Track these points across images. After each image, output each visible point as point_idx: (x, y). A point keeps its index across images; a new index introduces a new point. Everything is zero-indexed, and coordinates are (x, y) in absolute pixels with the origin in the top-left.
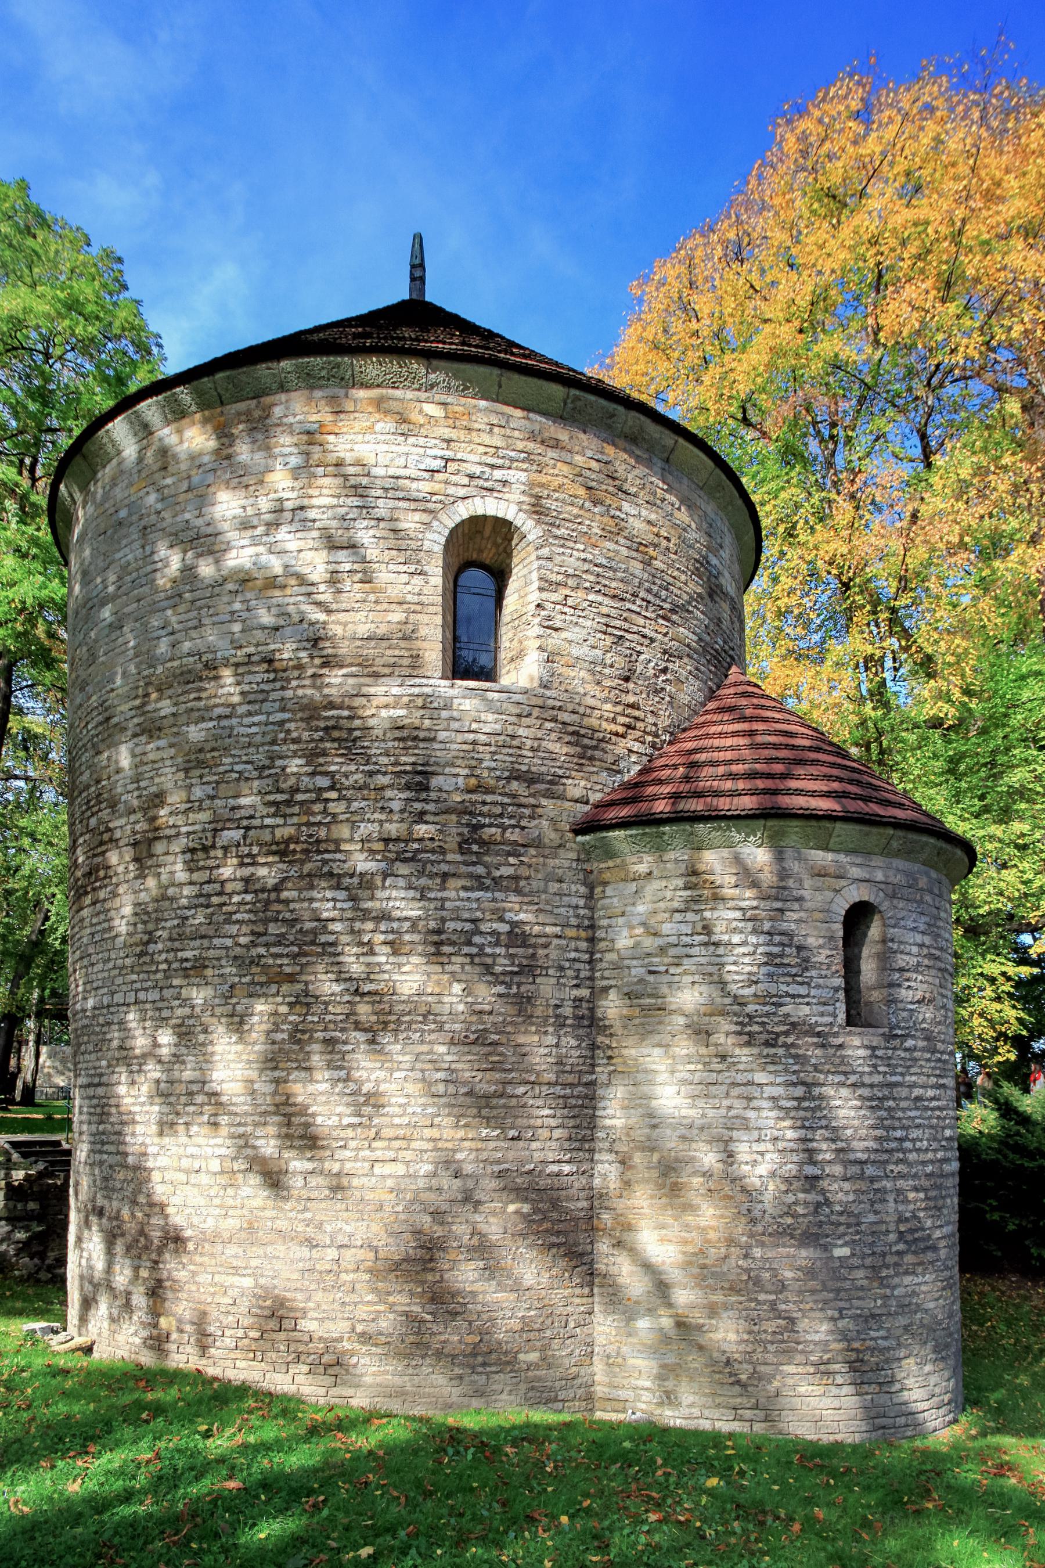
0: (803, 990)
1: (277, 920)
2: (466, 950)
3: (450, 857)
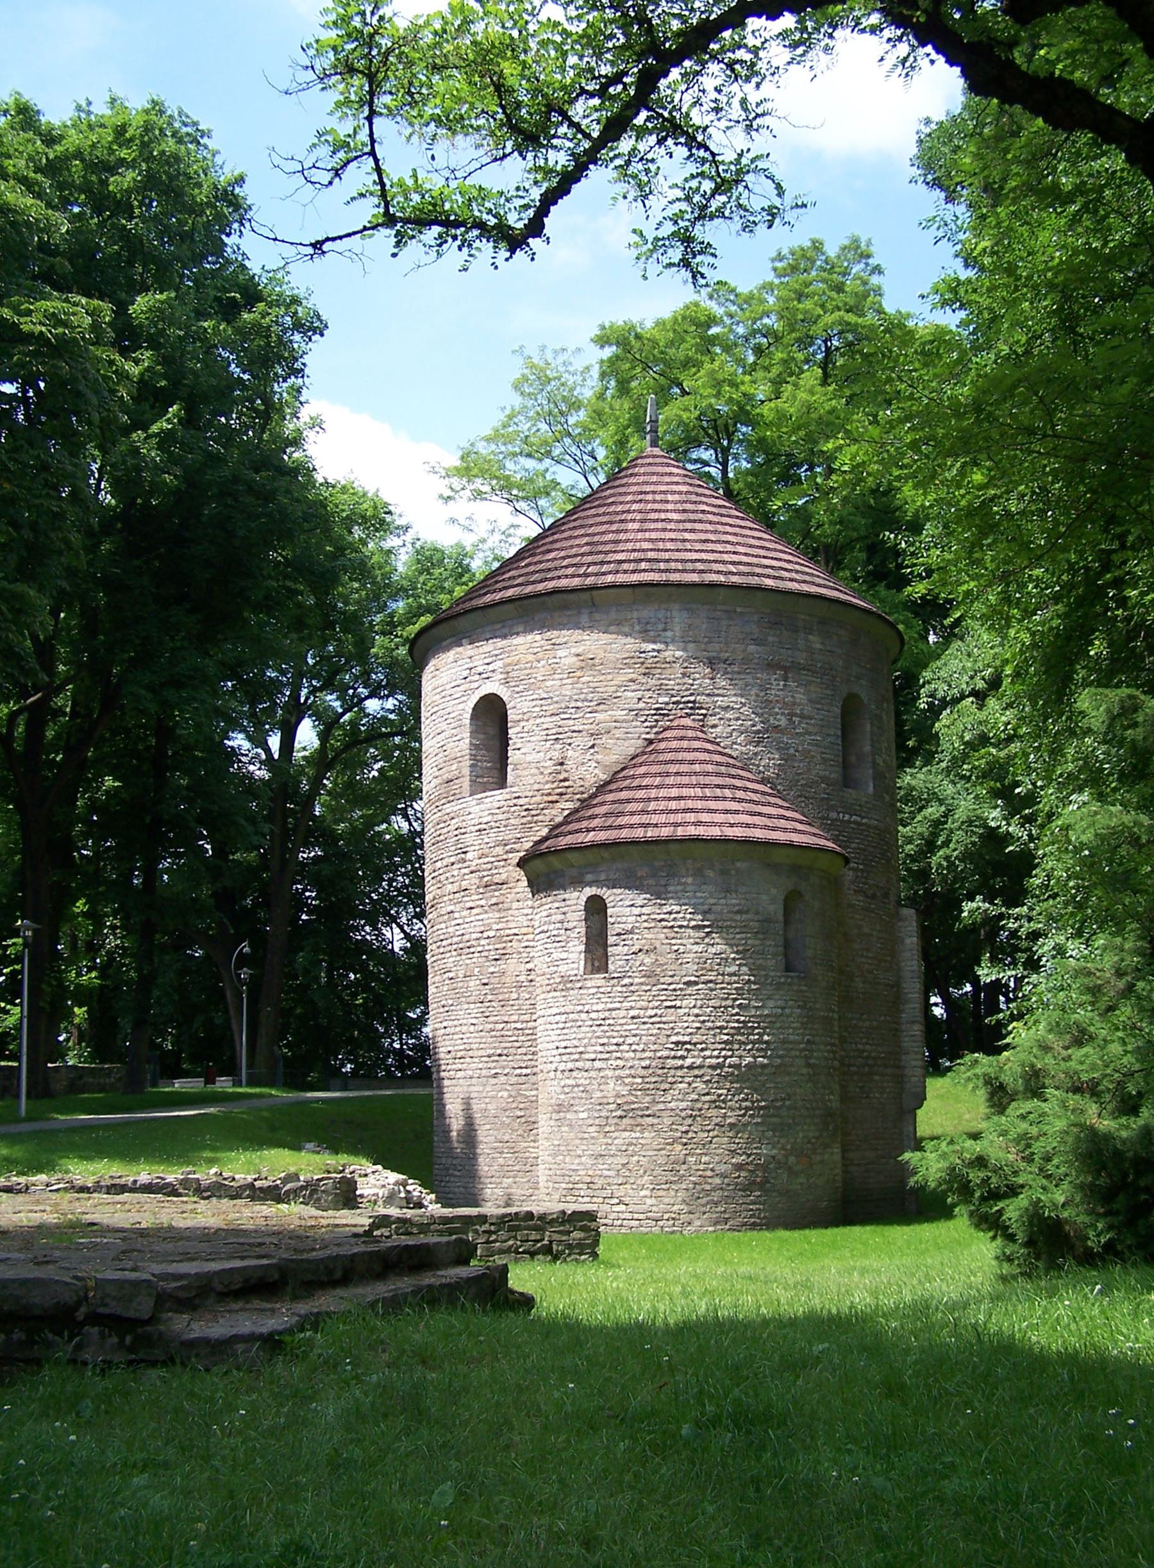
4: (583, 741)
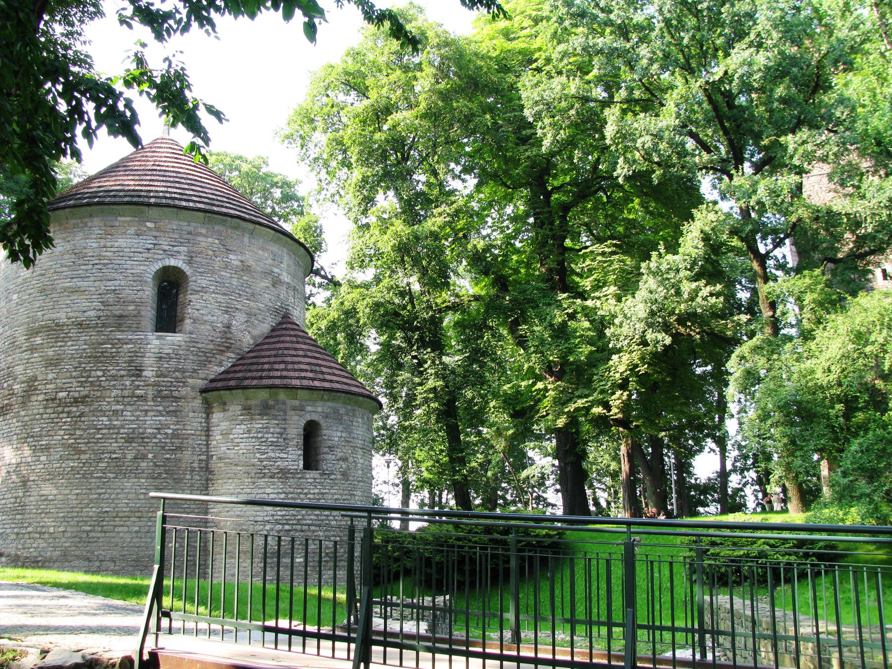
0: (285, 456)
1: (79, 429)
2: (154, 440)
3: (149, 403)
4: (241, 317)
